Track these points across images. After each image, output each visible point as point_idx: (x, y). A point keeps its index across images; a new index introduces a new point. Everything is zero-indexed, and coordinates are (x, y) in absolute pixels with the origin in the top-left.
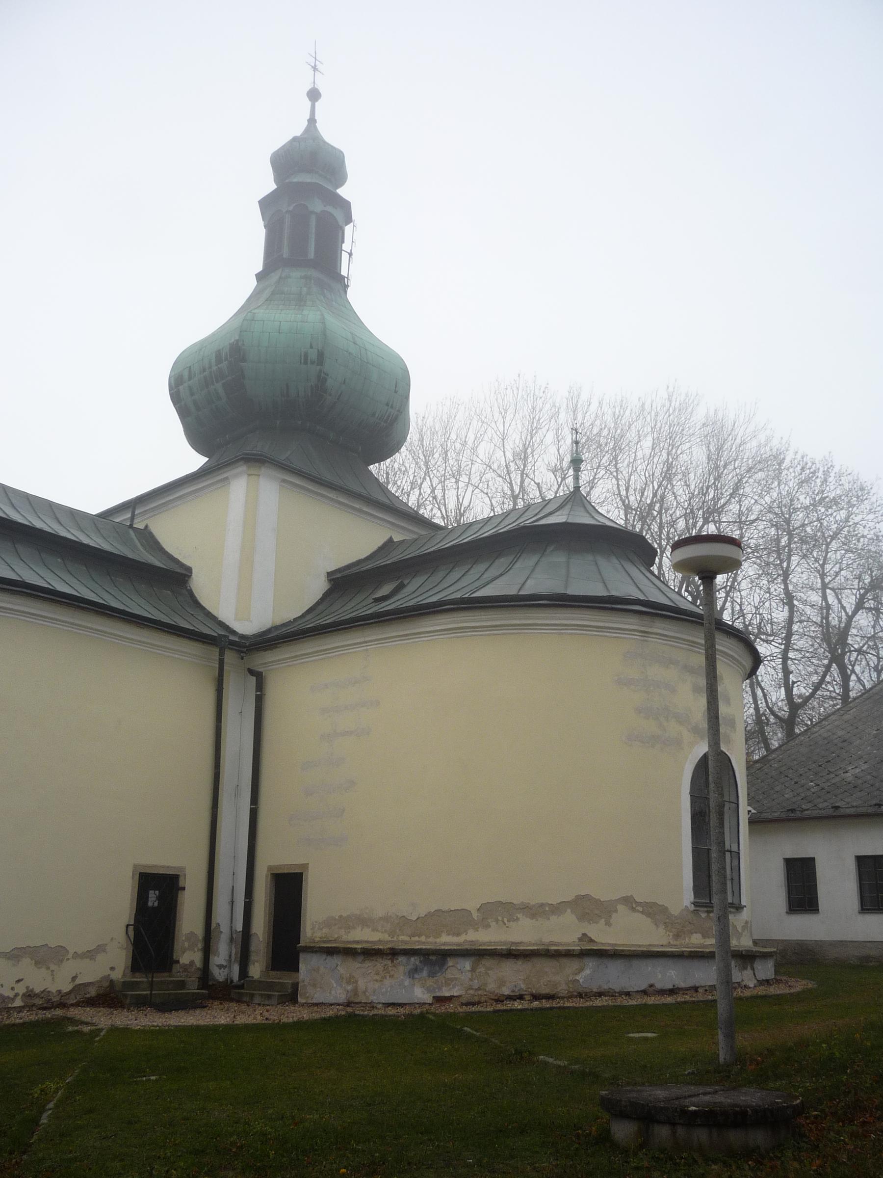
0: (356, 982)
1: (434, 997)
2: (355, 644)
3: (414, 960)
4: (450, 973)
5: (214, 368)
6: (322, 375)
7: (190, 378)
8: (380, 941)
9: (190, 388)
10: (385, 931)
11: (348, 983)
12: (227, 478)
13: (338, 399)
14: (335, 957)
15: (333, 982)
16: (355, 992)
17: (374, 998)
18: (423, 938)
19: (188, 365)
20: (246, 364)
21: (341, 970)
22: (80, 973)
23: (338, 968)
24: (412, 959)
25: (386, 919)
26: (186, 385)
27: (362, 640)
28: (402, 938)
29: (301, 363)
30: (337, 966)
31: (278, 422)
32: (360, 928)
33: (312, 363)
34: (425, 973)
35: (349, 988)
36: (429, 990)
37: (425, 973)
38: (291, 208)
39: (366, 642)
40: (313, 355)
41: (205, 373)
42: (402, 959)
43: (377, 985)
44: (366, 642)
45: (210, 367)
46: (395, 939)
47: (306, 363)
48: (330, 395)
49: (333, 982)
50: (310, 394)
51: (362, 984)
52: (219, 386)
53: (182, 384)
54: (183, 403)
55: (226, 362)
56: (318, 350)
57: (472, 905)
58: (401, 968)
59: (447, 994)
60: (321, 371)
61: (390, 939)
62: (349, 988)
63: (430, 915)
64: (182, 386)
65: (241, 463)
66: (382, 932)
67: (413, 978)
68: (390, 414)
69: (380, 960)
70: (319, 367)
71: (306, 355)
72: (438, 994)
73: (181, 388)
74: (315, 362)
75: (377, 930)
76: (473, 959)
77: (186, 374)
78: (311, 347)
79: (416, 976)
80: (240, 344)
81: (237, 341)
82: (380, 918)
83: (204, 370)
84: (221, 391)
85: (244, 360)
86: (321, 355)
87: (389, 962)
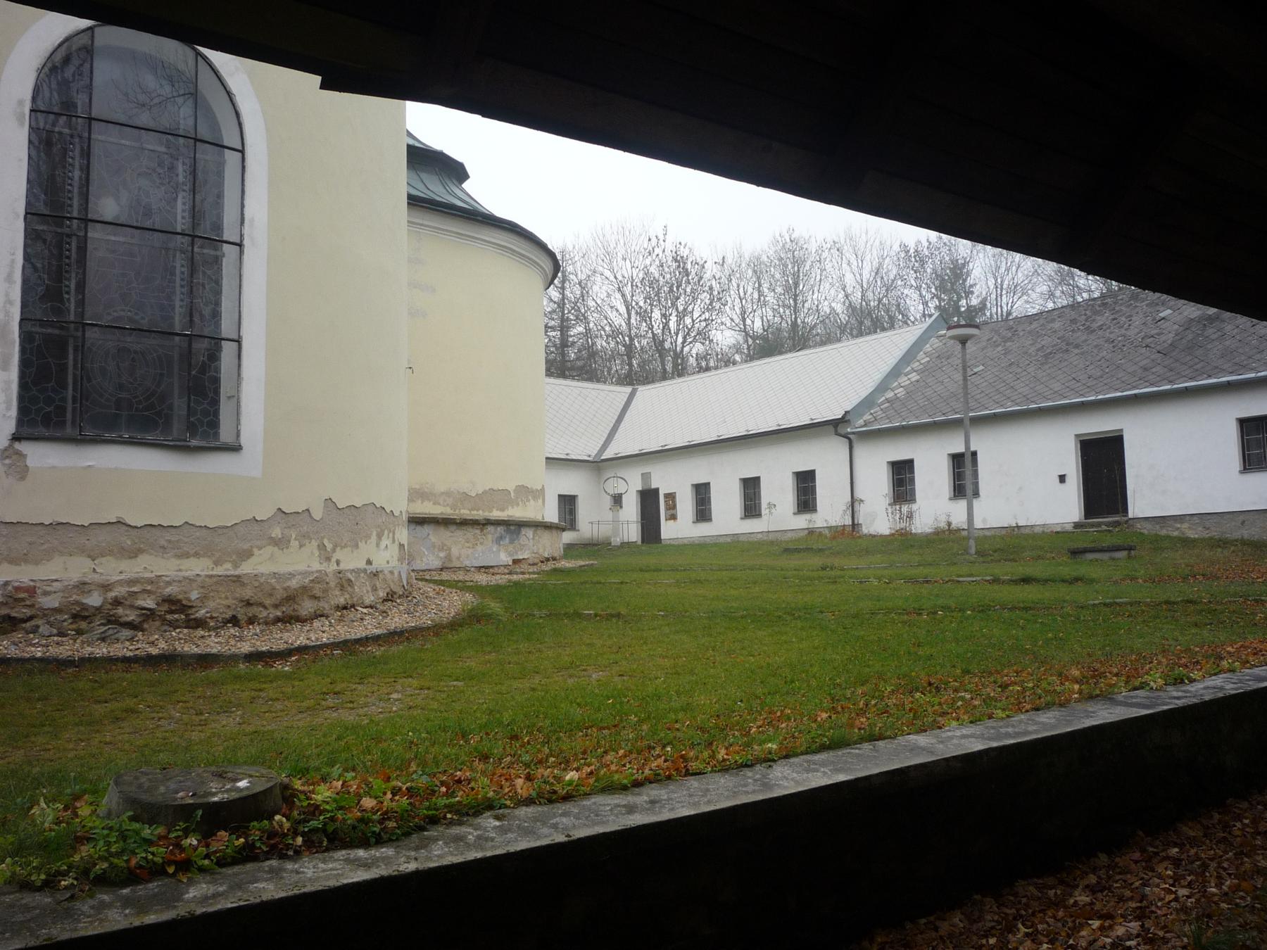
0: (450, 549)
1: (513, 560)
2: (447, 230)
3: (500, 529)
4: (523, 540)
8: (442, 513)
10: (448, 505)
11: (441, 549)
14: (426, 526)
15: (424, 550)
16: (448, 558)
17: (467, 563)
18: (481, 512)
21: (433, 539)
23: (431, 537)
24: (499, 529)
25: (448, 494)
27: (421, 222)
28: (462, 511)
30: (429, 535)
32: (420, 501)
34: (507, 540)
35: (442, 555)
36: (510, 555)
37: (507, 540)
39: (422, 225)
42: (490, 528)
43: (470, 551)
44: (422, 225)
46: (457, 512)
49: (424, 550)
51: (455, 551)
57: (511, 487)
58: (490, 537)
59: (521, 557)
61: (452, 512)
62: (442, 555)
63: (485, 492)
66: (444, 506)
67: (500, 545)
69: (471, 530)
72: (516, 558)
75: (439, 504)
76: (533, 529)
79: (501, 543)
82: (443, 493)
87: (478, 532)
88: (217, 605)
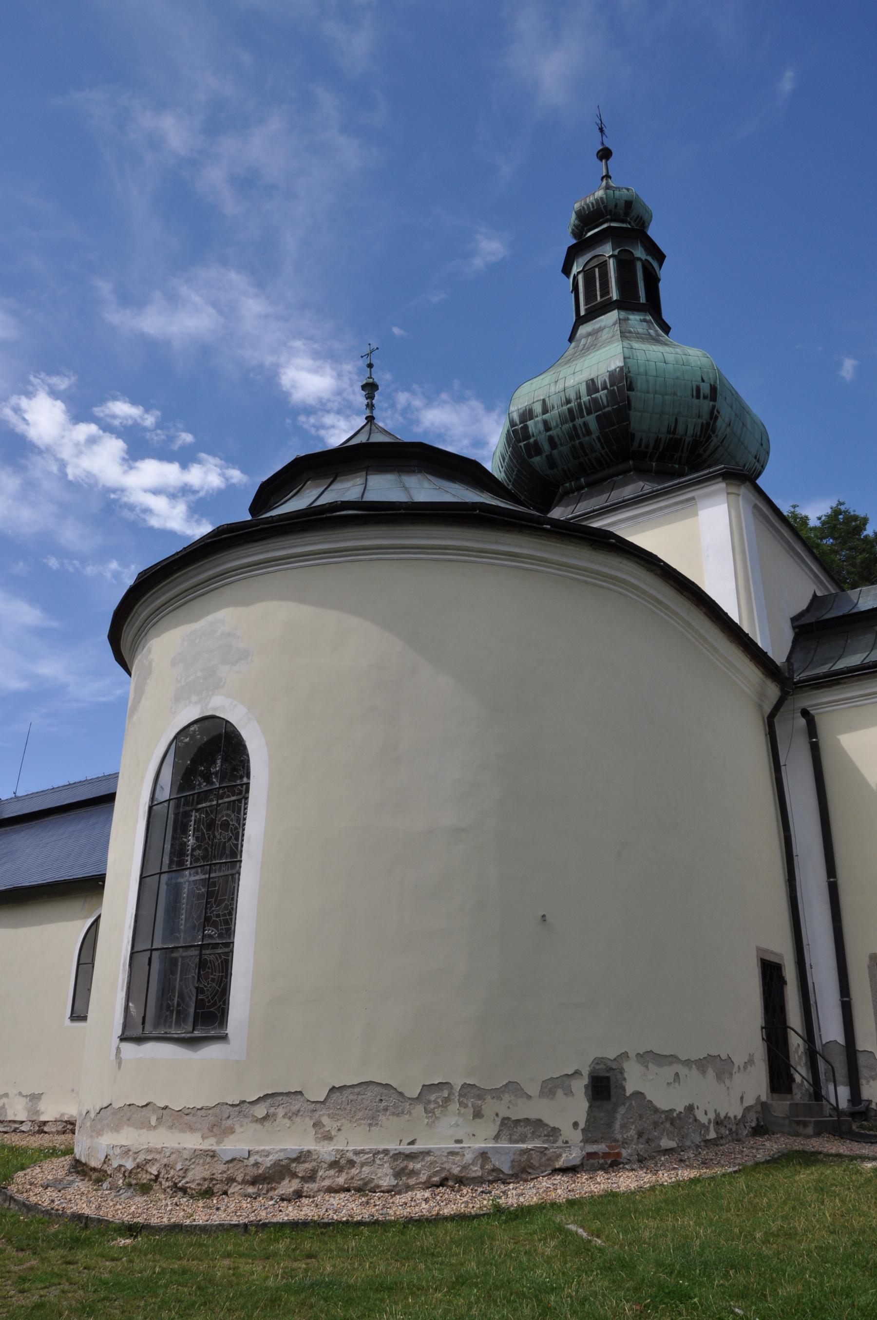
5: (585, 398)
6: (715, 412)
7: (545, 411)
9: (545, 422)
12: (693, 498)
13: (722, 442)
19: (542, 398)
20: (633, 393)
22: (509, 1108)
26: (539, 419)
29: (693, 397)
31: (654, 464)
33: (705, 397)
38: (616, 253)
40: (705, 389)
41: (569, 406)
45: (579, 397)
47: (698, 397)
48: (717, 436)
50: (699, 433)
52: (591, 420)
53: (531, 418)
54: (532, 440)
55: (605, 391)
56: (711, 385)
60: (714, 407)
64: (532, 421)
65: (720, 479)
68: (756, 468)
70: (711, 403)
71: (698, 389)
73: (530, 423)
74: (707, 396)
77: (538, 408)
78: (703, 381)
80: (625, 370)
81: (621, 368)
83: (568, 401)
84: (593, 425)
85: (630, 388)
86: (713, 389)
88: (197, 1174)
